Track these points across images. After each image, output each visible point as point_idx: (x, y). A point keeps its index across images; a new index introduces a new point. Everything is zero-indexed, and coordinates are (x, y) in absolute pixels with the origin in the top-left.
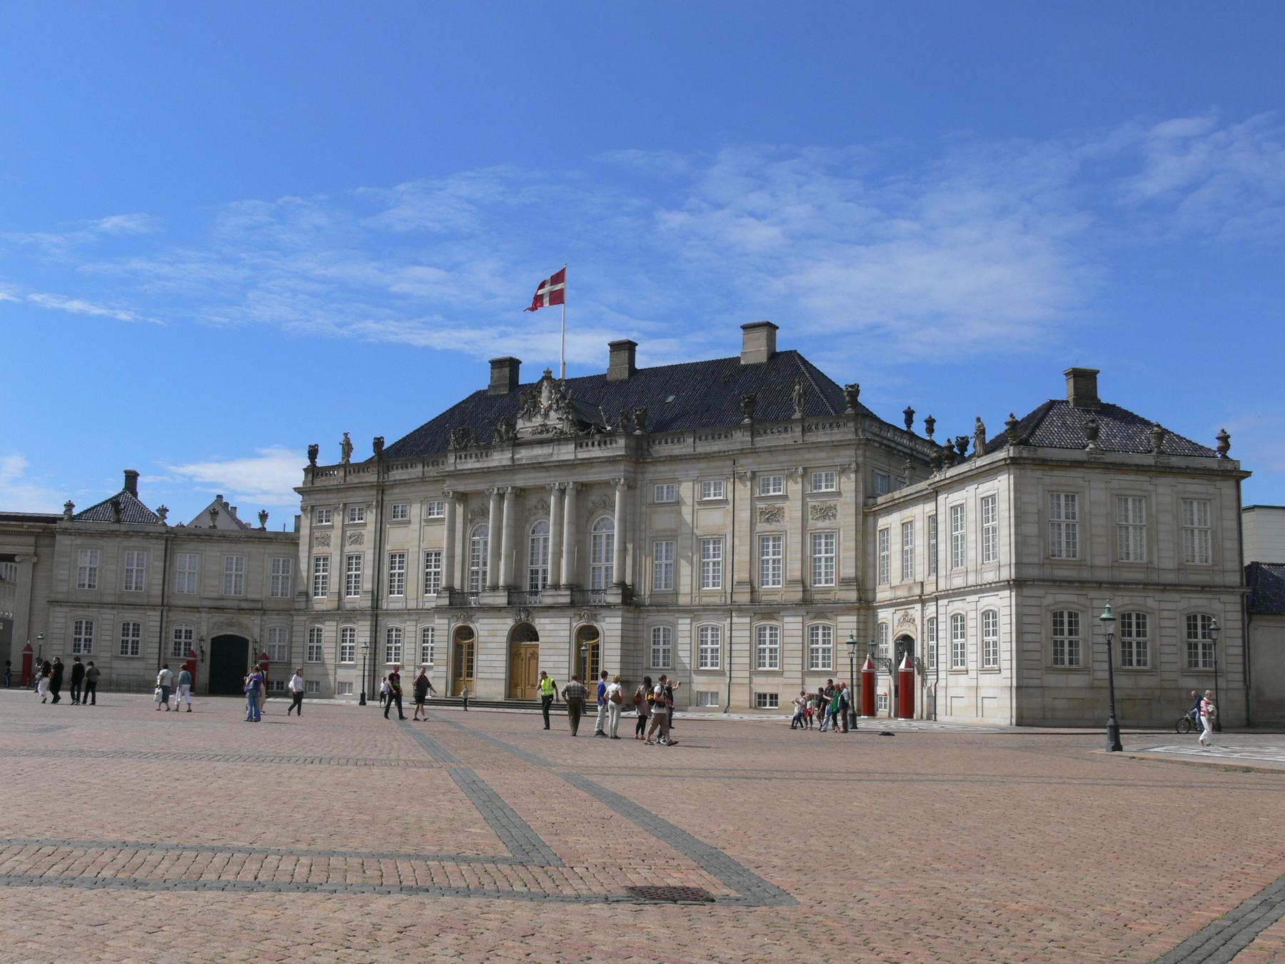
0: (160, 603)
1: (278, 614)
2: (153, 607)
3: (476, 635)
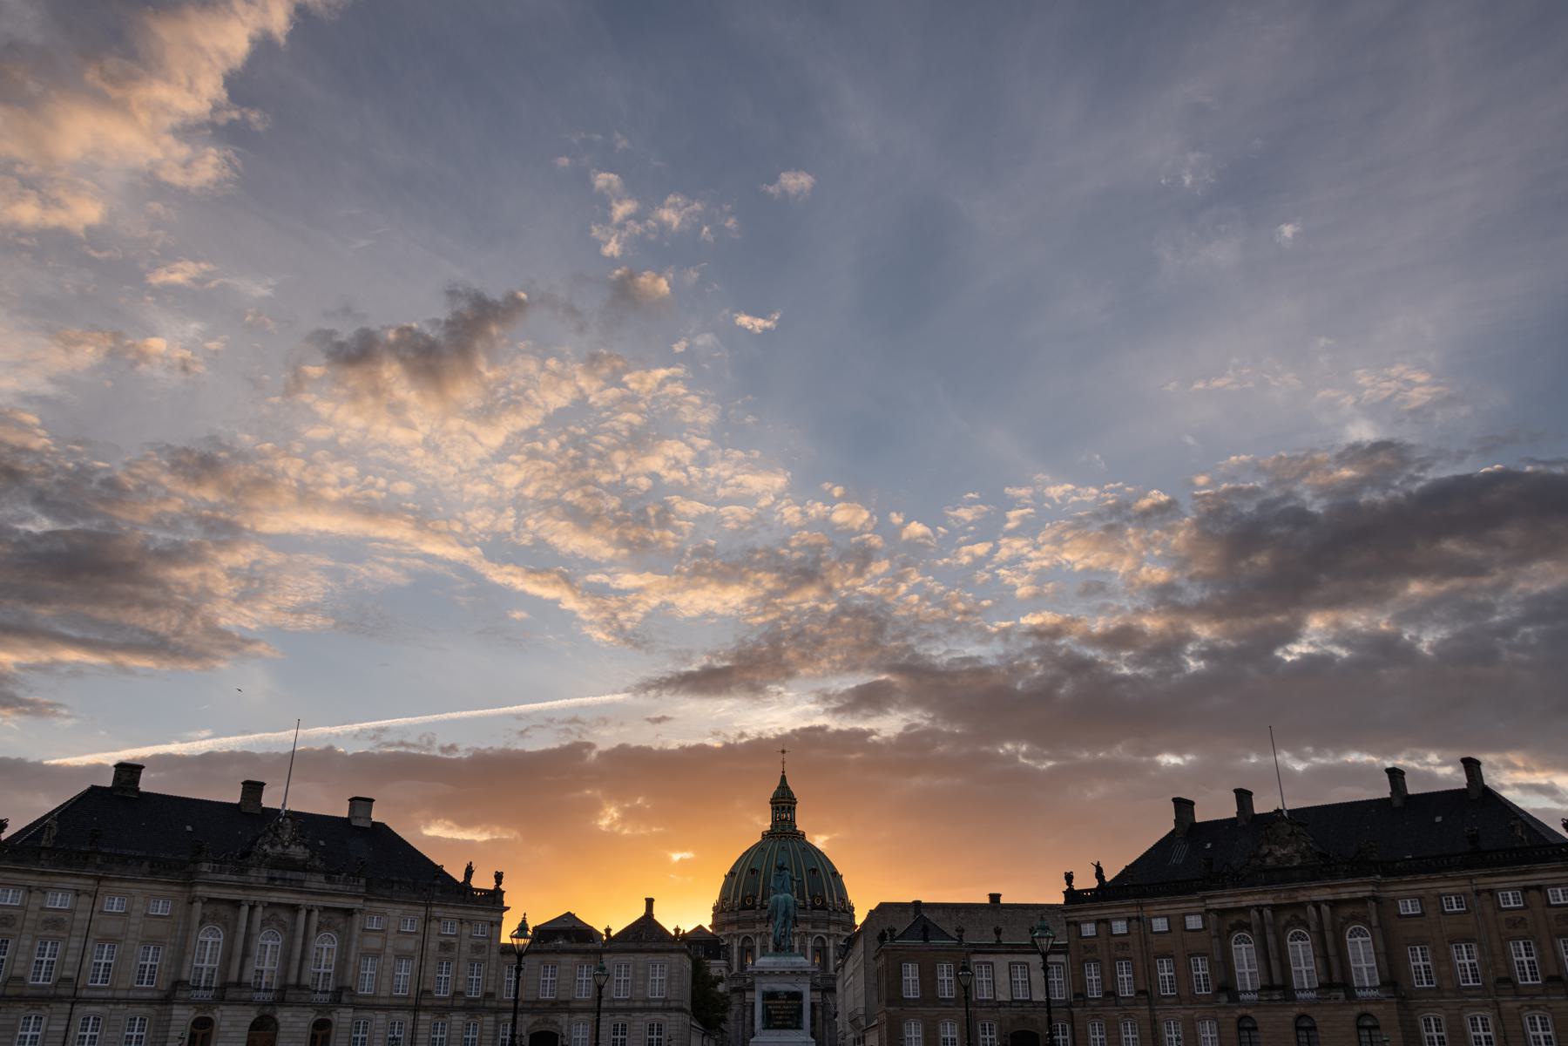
3: (216, 1025)
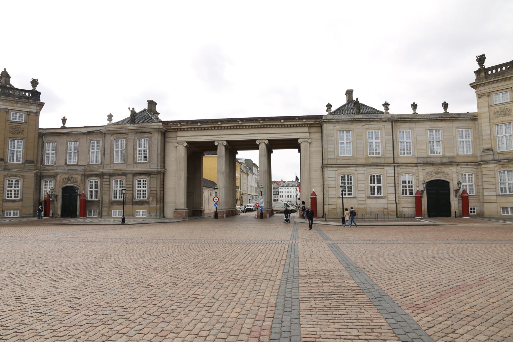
0: (393, 163)
1: (467, 165)
2: (389, 165)
